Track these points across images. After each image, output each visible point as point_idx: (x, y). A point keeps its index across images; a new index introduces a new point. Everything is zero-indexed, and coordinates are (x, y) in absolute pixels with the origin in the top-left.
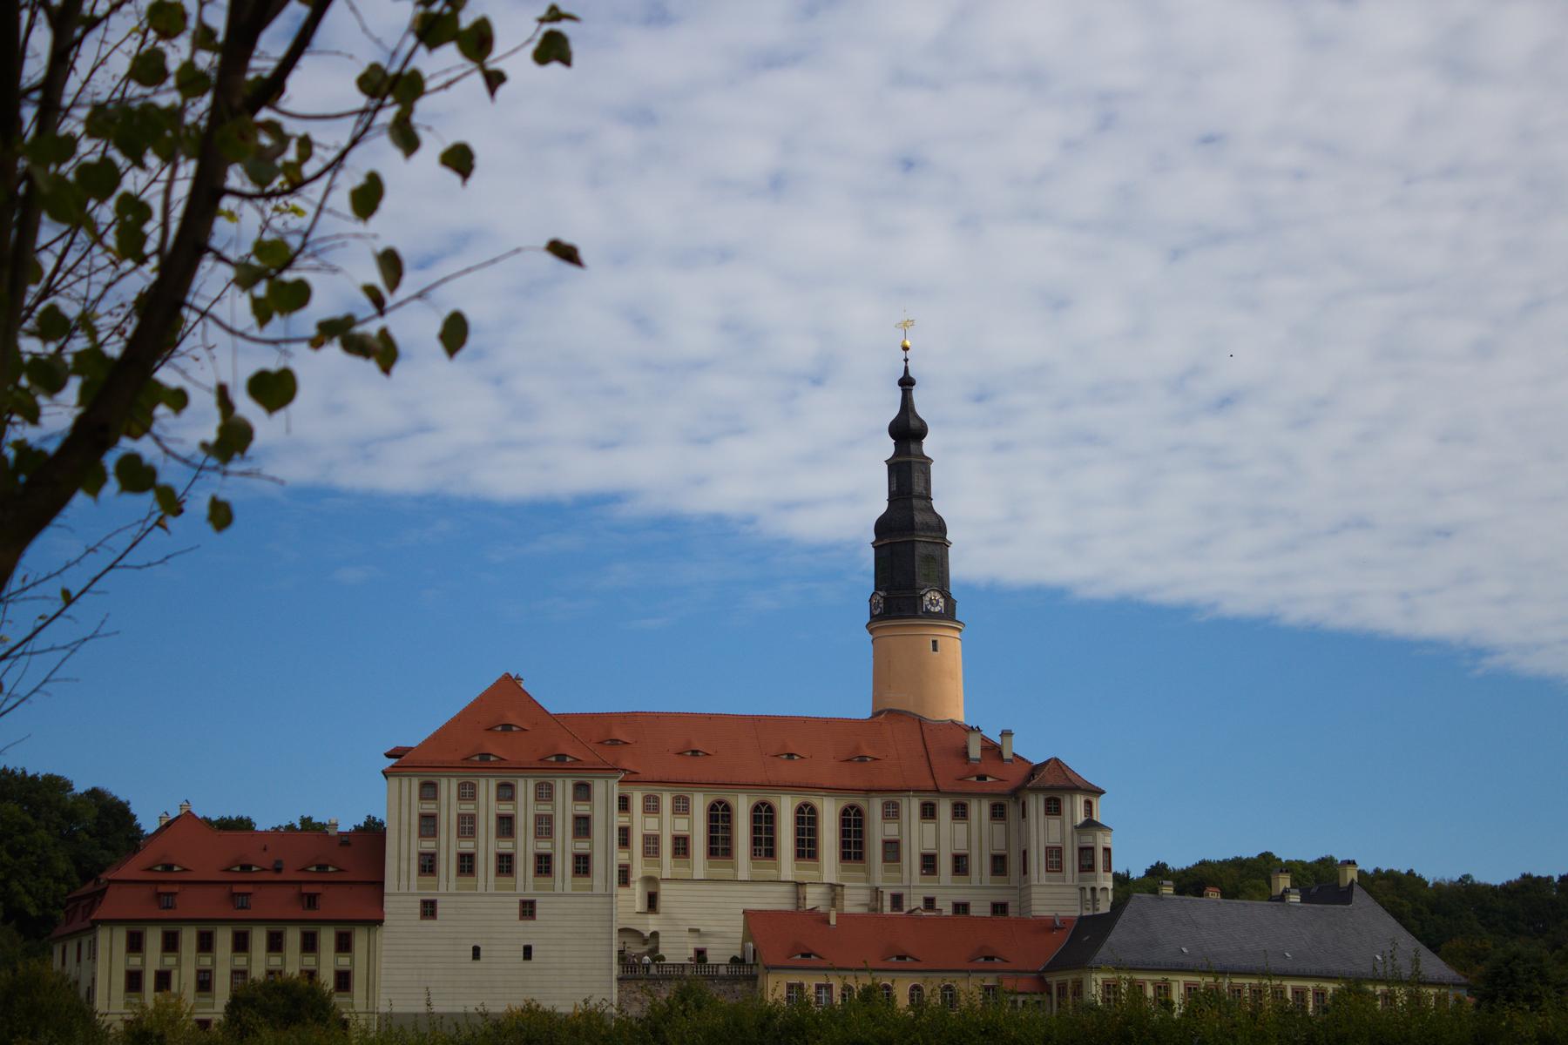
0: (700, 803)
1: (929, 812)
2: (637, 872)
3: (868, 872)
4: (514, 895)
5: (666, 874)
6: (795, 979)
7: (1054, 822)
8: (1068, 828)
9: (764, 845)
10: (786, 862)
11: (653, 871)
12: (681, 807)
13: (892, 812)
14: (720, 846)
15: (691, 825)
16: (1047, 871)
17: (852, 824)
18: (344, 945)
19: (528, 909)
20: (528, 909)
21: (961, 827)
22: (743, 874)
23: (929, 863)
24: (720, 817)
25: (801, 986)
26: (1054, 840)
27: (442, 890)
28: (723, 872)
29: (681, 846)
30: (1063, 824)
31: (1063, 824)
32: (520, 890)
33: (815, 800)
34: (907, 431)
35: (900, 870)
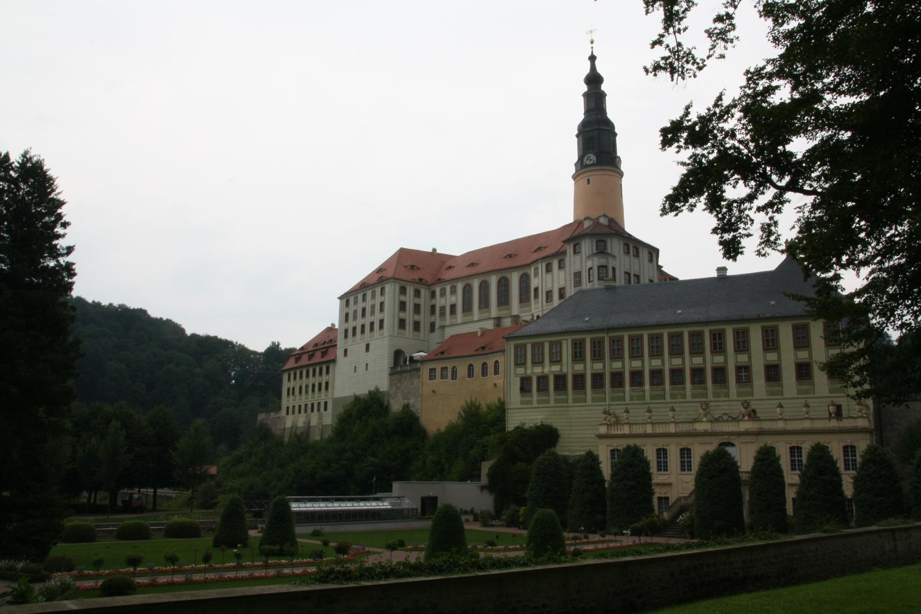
0: (460, 287)
1: (549, 269)
2: (437, 325)
3: (530, 306)
4: (363, 342)
5: (448, 324)
6: (432, 365)
7: (578, 257)
8: (584, 258)
9: (484, 303)
10: (494, 311)
11: (443, 323)
12: (454, 291)
13: (536, 274)
14: (467, 308)
15: (457, 298)
16: (575, 287)
17: (525, 281)
18: (328, 372)
19: (368, 346)
20: (368, 346)
21: (562, 273)
22: (476, 318)
23: (549, 294)
24: (467, 290)
25: (435, 369)
26: (577, 268)
27: (349, 344)
28: (468, 318)
29: (453, 307)
30: (581, 259)
31: (581, 259)
32: (366, 340)
33: (507, 275)
34: (594, 80)
35: (538, 303)
